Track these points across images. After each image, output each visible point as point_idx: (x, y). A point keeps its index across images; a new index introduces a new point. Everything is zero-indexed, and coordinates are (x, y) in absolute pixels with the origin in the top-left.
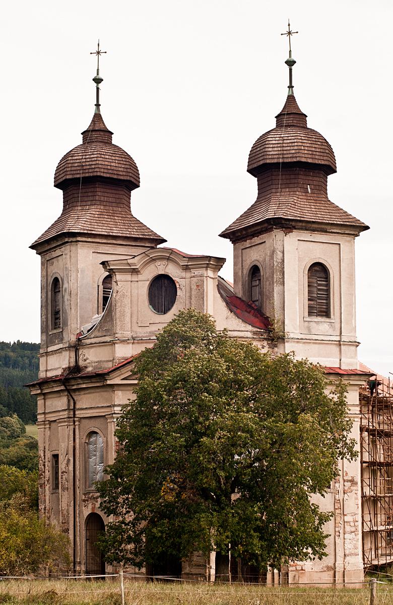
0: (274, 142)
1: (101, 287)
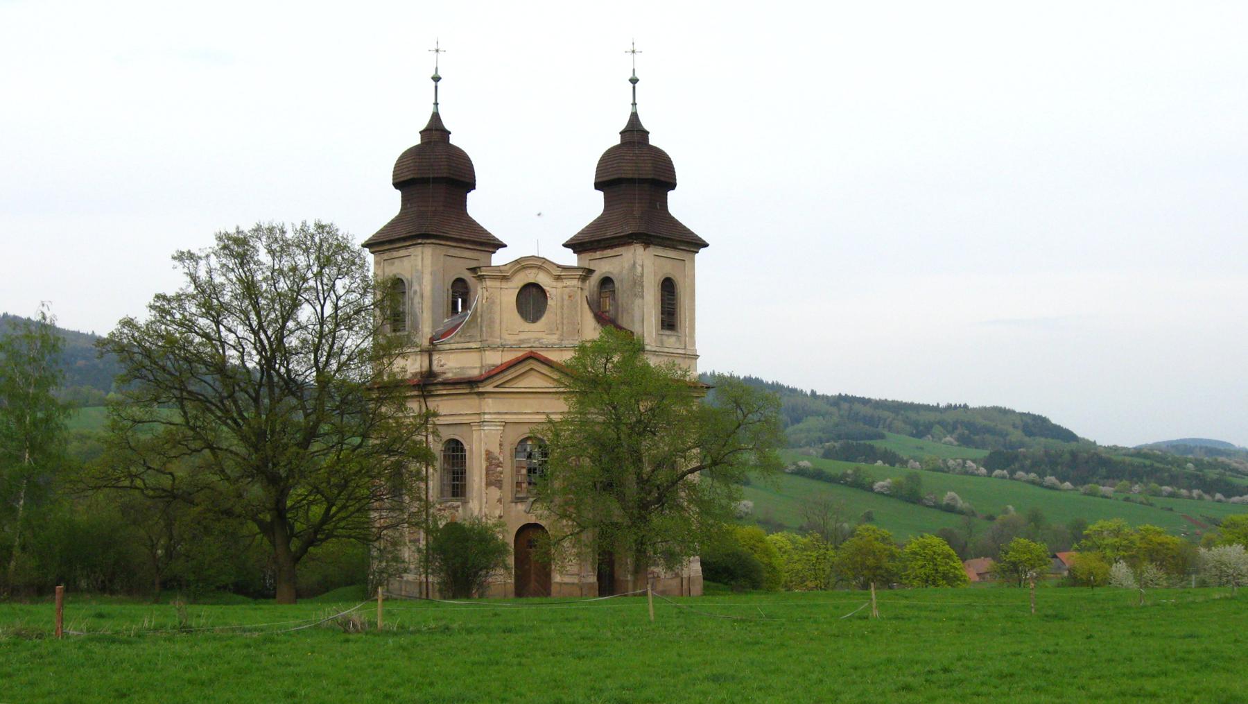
0: (628, 158)
1: (451, 291)
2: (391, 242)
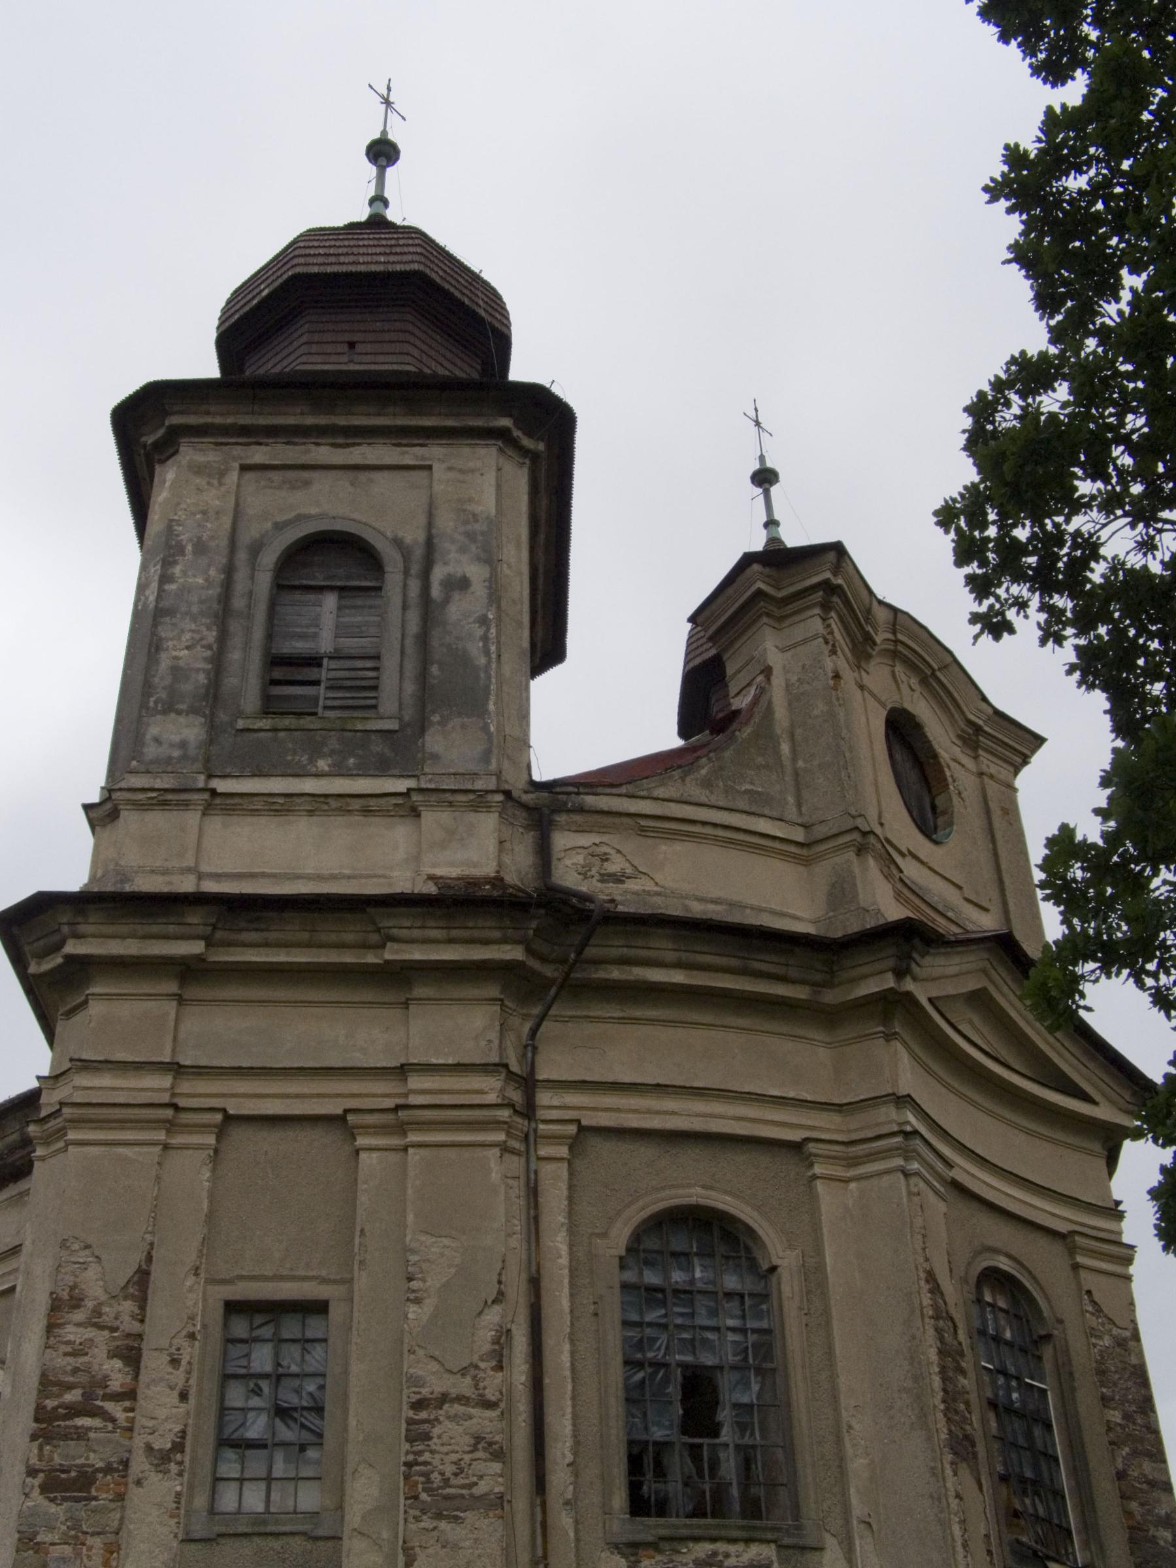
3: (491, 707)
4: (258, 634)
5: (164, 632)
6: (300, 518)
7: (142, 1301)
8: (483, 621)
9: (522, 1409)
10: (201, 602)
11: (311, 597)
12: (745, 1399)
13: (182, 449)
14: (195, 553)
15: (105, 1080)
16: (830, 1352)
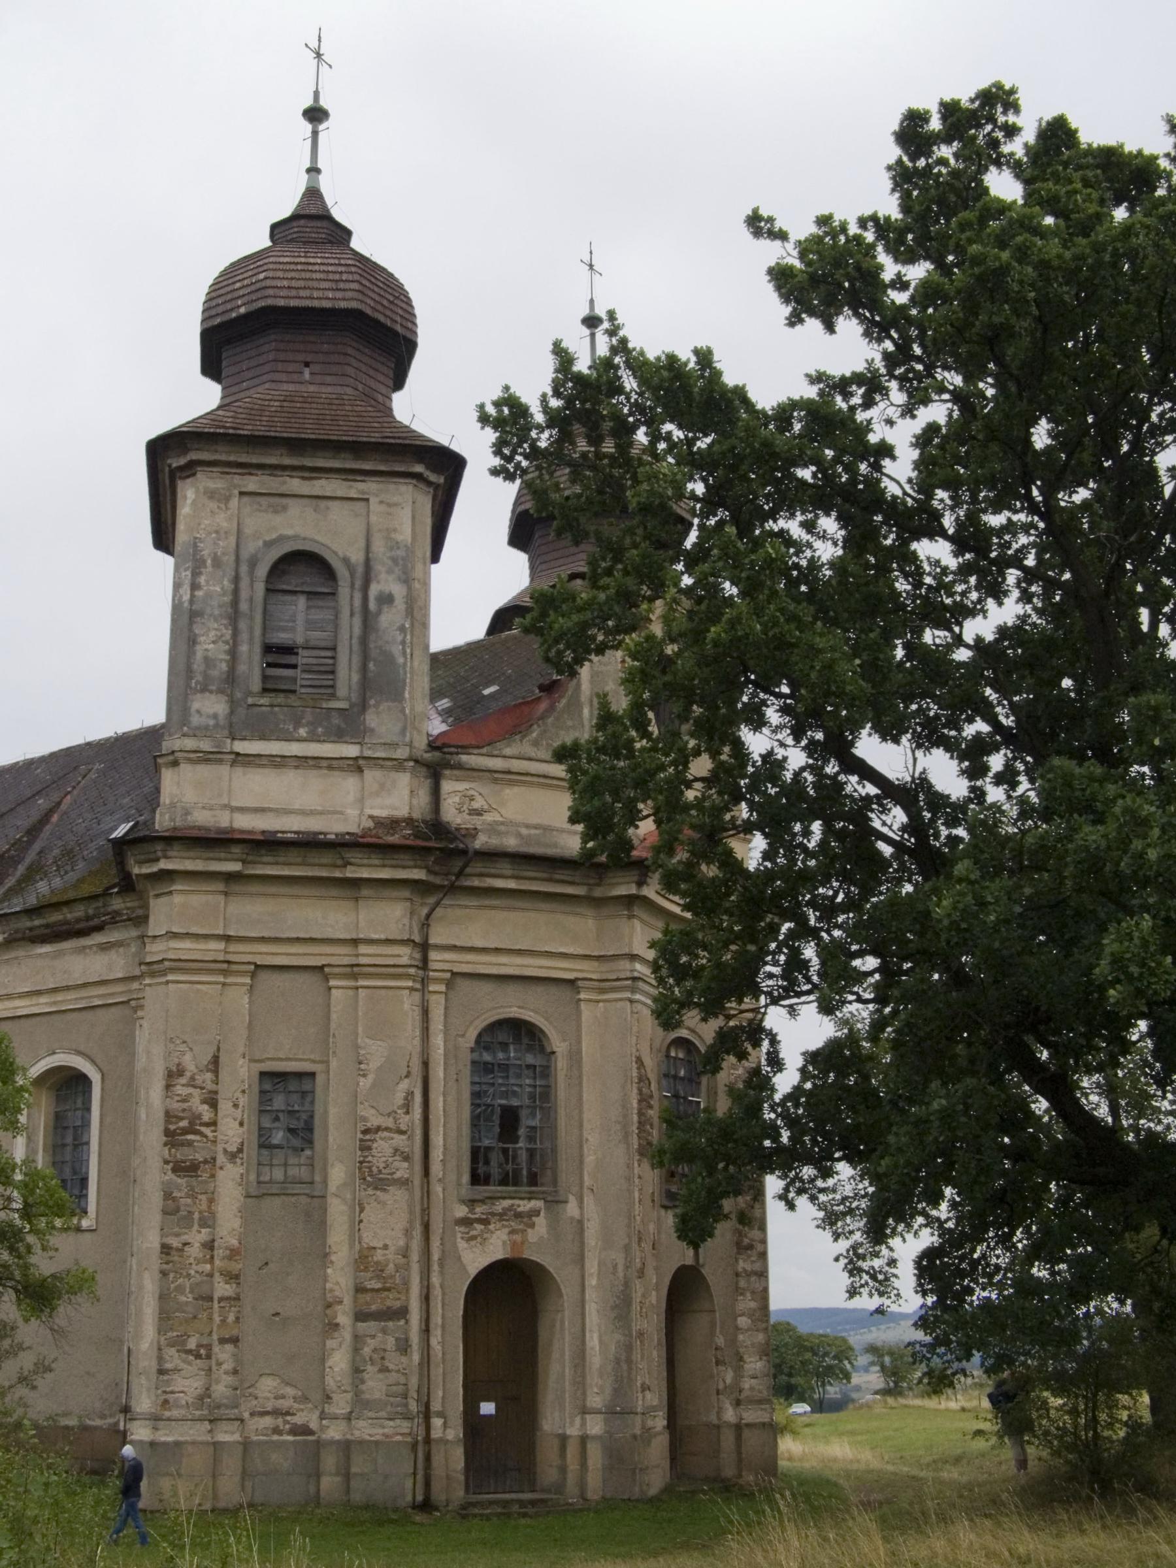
2: (296, 445)
3: (407, 695)
4: (258, 632)
5: (197, 630)
6: (281, 539)
7: (216, 1072)
8: (402, 629)
9: (418, 1132)
10: (220, 606)
11: (288, 598)
12: (533, 1124)
13: (199, 475)
14: (213, 566)
15: (187, 944)
16: (580, 1099)
